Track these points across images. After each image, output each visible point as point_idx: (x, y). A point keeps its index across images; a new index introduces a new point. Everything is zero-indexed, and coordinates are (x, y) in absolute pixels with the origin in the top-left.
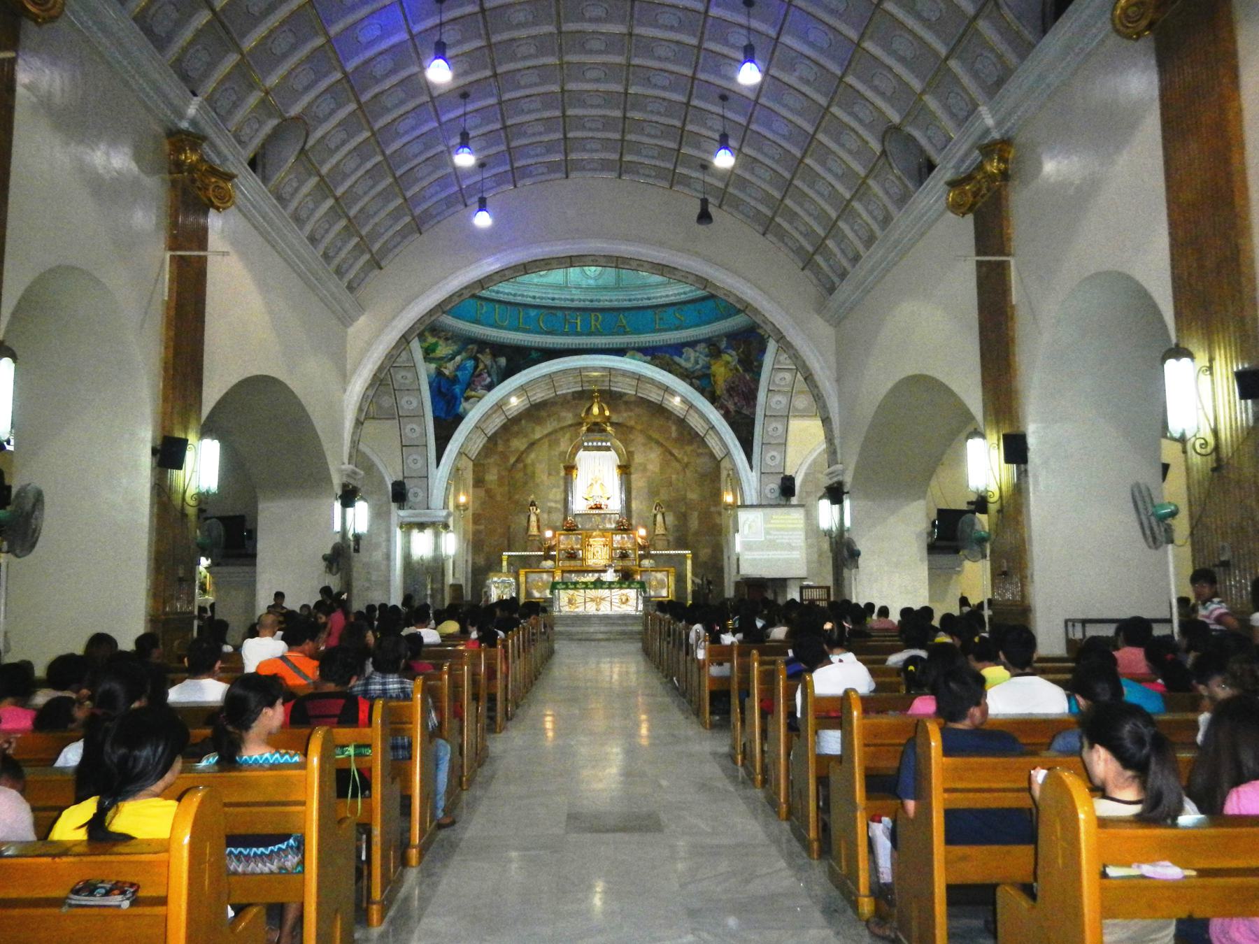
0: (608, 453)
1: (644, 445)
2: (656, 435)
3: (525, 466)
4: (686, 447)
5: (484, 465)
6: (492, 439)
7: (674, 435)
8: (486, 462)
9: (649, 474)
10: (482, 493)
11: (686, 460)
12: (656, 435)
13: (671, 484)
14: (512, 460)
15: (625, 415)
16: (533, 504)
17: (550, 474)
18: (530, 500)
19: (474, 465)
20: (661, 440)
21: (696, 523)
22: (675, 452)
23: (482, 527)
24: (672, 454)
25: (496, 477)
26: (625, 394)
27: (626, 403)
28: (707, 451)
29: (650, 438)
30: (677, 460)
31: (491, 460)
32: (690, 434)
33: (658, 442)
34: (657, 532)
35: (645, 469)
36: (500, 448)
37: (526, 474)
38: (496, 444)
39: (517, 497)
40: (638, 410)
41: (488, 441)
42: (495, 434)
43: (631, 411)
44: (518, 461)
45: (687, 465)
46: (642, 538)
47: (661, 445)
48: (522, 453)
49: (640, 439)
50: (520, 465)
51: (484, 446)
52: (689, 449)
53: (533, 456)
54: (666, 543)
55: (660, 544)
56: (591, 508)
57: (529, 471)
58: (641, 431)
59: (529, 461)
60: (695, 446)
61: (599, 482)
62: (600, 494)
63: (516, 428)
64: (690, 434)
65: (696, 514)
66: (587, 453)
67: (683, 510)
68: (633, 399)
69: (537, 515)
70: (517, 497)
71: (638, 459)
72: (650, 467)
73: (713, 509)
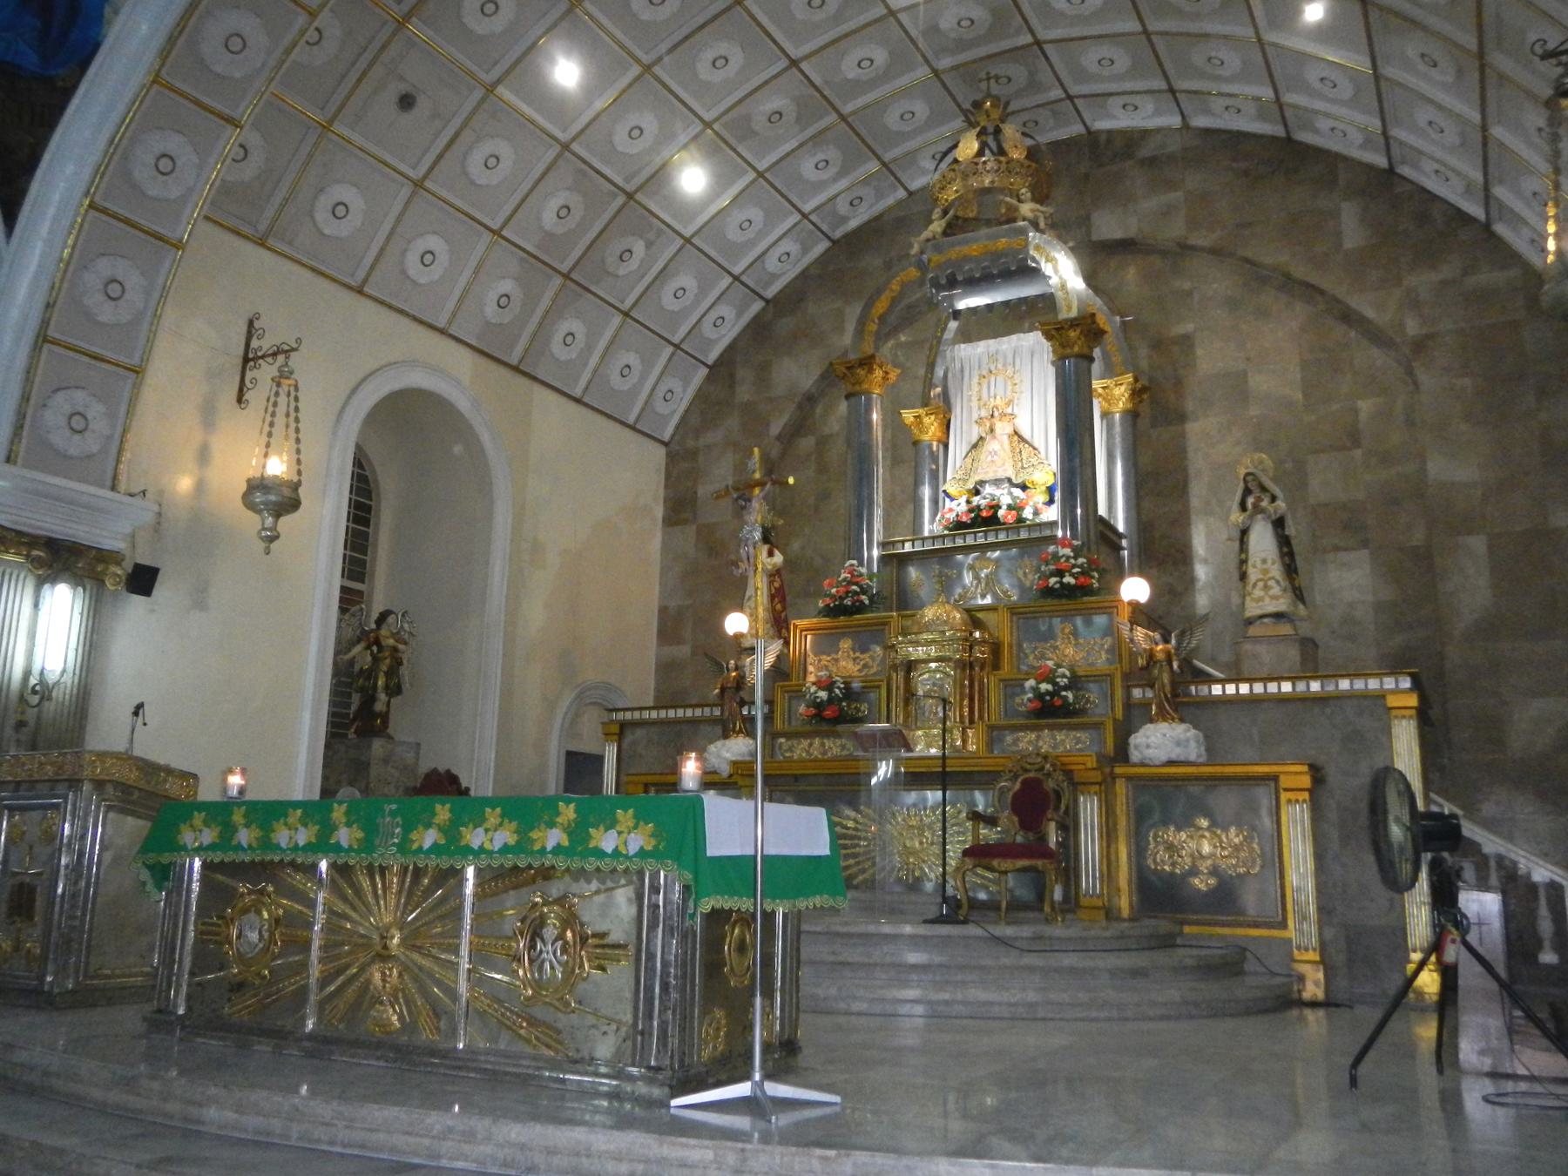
1: (1232, 304)
2: (1273, 255)
3: (823, 442)
4: (1411, 280)
5: (693, 454)
6: (723, 370)
8: (702, 442)
9: (1254, 411)
10: (687, 538)
11: (1412, 327)
12: (1273, 255)
13: (1354, 439)
14: (775, 429)
15: (1151, 204)
19: (668, 455)
20: (1300, 271)
23: (683, 651)
24: (1348, 317)
26: (1145, 133)
27: (1152, 162)
28: (1514, 273)
29: (1257, 276)
30: (1375, 336)
31: (711, 437)
33: (1291, 285)
34: (1252, 610)
35: (1236, 388)
36: (744, 393)
37: (822, 469)
38: (732, 382)
40: (1194, 180)
41: (708, 378)
42: (732, 348)
43: (1171, 185)
44: (797, 429)
45: (1420, 346)
46: (1140, 614)
47: (1311, 291)
49: (1217, 283)
50: (807, 443)
51: (700, 396)
52: (1422, 281)
54: (1293, 654)
55: (1265, 655)
56: (959, 525)
58: (1215, 252)
61: (1003, 428)
63: (786, 325)
65: (1478, 544)
66: (981, 348)
67: (1418, 537)
68: (1174, 146)
71: (1211, 358)
72: (1260, 382)
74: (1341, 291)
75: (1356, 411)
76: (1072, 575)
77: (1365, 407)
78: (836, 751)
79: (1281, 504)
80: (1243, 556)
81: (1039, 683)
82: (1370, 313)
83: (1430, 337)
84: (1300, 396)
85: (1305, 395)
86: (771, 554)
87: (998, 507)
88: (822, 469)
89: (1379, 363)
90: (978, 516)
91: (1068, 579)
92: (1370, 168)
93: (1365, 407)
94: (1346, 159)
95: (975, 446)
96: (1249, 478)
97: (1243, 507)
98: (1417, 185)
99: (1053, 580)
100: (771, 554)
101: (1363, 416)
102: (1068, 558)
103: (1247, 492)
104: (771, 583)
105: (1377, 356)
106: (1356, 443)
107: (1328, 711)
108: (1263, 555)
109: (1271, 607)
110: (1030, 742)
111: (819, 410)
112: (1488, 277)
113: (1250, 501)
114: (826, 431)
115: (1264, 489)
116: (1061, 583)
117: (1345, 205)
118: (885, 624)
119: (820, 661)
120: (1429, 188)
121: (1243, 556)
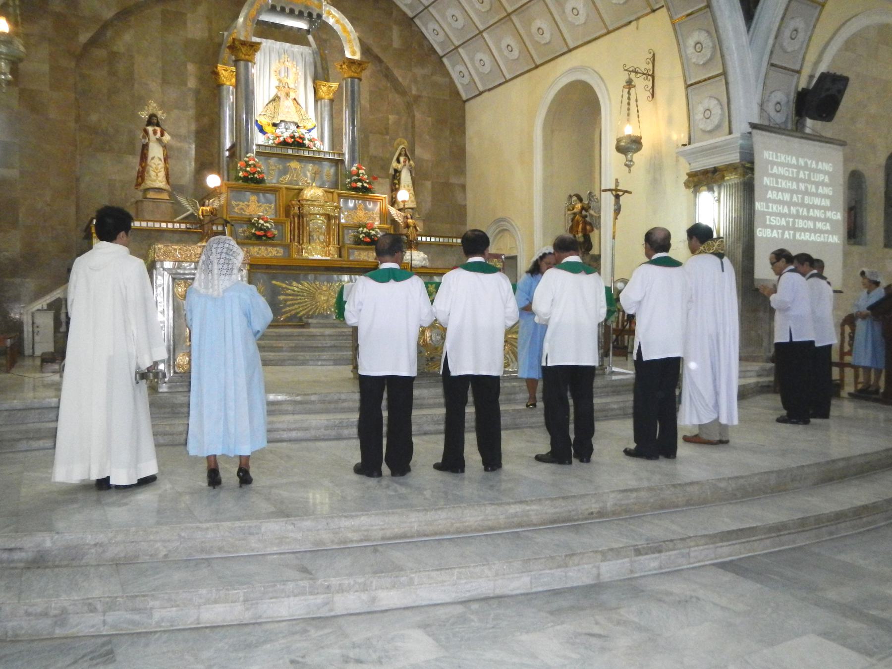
0: (297, 48)
7: (397, 43)
11: (414, 92)
14: (84, 37)
16: (152, 120)
17: (165, 81)
18: (144, 115)
21: (429, 199)
22: (398, 73)
25: (46, 68)
28: (447, 80)
32: (421, 45)
37: (113, 73)
39: (94, 118)
45: (417, 98)
48: (106, 26)
50: (100, 53)
52: (419, 71)
53: (128, 37)
56: (285, 143)
57: (121, 67)
59: (120, 46)
60: (427, 71)
62: (296, 120)
64: (421, 45)
69: (165, 147)
70: (94, 118)
73: (454, 180)
74: (391, 65)
75: (388, 119)
76: (366, 182)
77: (392, 118)
78: (274, 253)
79: (412, 162)
80: (396, 181)
81: (369, 230)
82: (400, 79)
83: (419, 96)
84: (368, 106)
85: (371, 106)
86: (162, 135)
87: (303, 139)
88: (113, 73)
89: (398, 100)
90: (295, 140)
91: (365, 185)
92: (405, 14)
93: (392, 118)
94: (397, 6)
95: (274, 100)
96: (403, 150)
97: (398, 161)
98: (420, 29)
99: (359, 184)
100: (162, 135)
101: (390, 122)
102: (362, 173)
103: (400, 155)
104: (164, 151)
105: (398, 99)
106: (387, 134)
107: (453, 249)
108: (408, 183)
109: (411, 206)
110: (365, 256)
111: (109, 33)
112: (438, 78)
113: (402, 159)
114: (115, 49)
115: (406, 155)
116: (363, 186)
117: (394, 27)
118: (277, 191)
119: (239, 205)
120: (425, 34)
121: (396, 181)
